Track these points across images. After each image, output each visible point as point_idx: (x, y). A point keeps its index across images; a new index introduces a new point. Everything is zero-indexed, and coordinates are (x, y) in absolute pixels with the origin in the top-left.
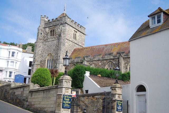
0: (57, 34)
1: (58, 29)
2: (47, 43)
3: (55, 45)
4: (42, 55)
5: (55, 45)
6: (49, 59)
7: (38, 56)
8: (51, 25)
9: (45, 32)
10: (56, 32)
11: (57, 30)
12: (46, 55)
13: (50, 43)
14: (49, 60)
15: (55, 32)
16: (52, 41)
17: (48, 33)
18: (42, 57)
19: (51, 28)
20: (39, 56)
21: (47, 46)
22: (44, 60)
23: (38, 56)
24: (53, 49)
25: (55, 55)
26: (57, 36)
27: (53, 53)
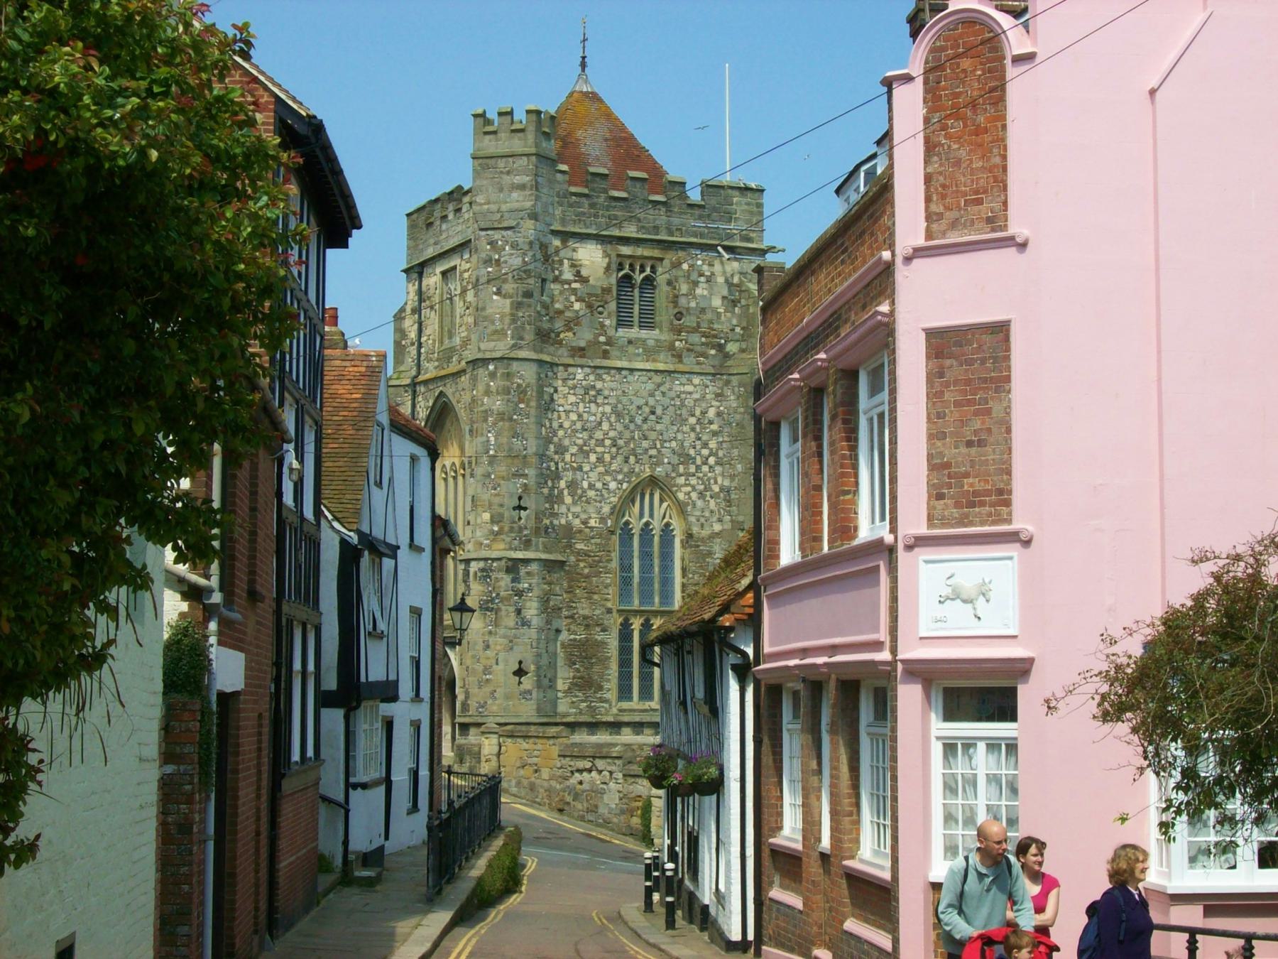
0: (689, 321)
1: (696, 284)
2: (607, 383)
3: (692, 420)
4: (572, 485)
5: (692, 420)
6: (657, 525)
7: (546, 491)
8: (630, 231)
9: (568, 275)
10: (683, 301)
11: (691, 293)
12: (613, 485)
13: (639, 386)
14: (656, 532)
15: (675, 300)
16: (658, 379)
17: (606, 291)
18: (568, 500)
19: (626, 250)
20: (550, 483)
21: (619, 415)
22: (592, 523)
23: (546, 491)
24: (674, 444)
25: (700, 503)
26: (696, 338)
27: (681, 480)
